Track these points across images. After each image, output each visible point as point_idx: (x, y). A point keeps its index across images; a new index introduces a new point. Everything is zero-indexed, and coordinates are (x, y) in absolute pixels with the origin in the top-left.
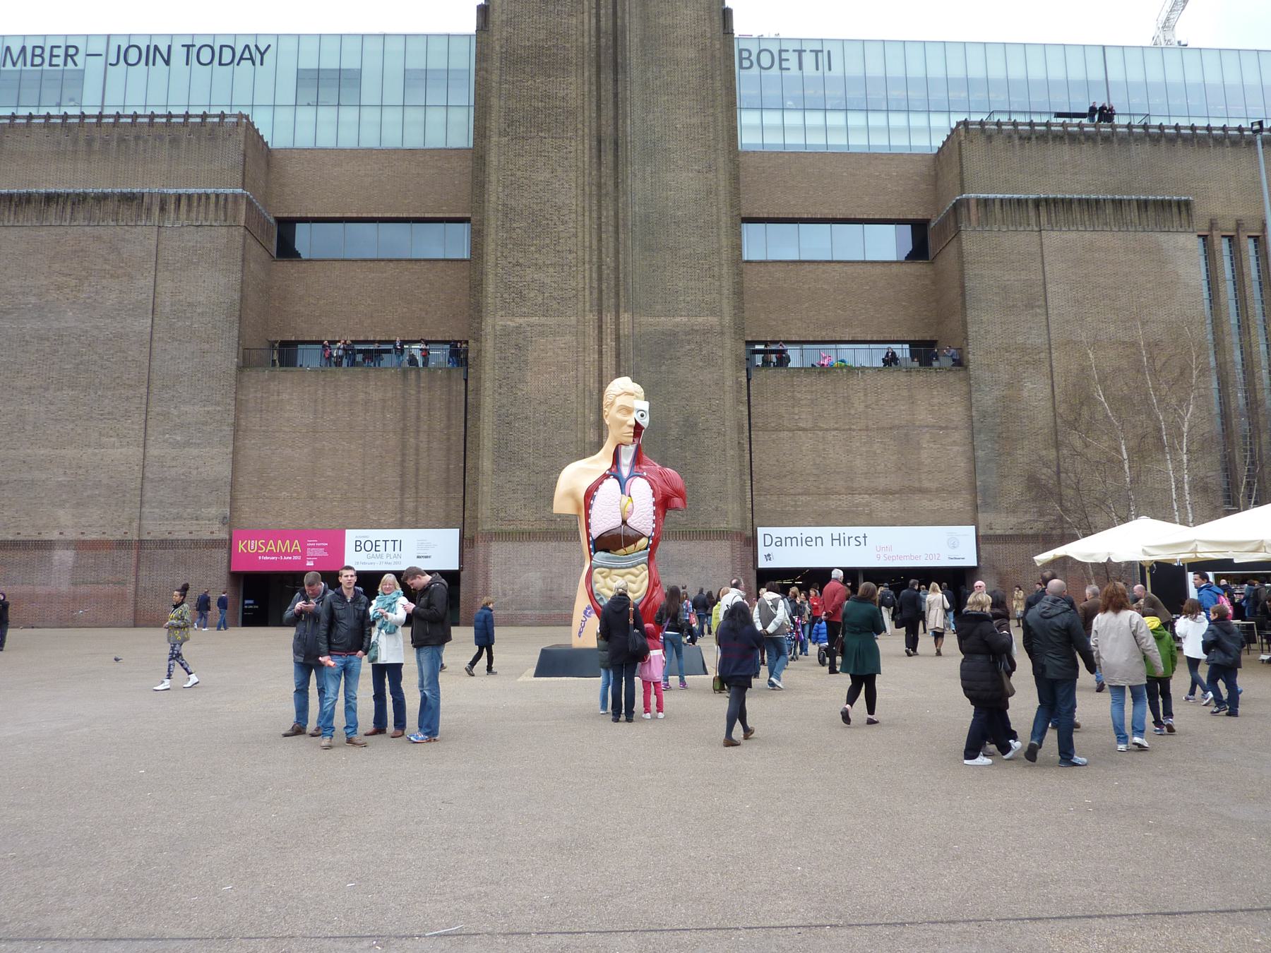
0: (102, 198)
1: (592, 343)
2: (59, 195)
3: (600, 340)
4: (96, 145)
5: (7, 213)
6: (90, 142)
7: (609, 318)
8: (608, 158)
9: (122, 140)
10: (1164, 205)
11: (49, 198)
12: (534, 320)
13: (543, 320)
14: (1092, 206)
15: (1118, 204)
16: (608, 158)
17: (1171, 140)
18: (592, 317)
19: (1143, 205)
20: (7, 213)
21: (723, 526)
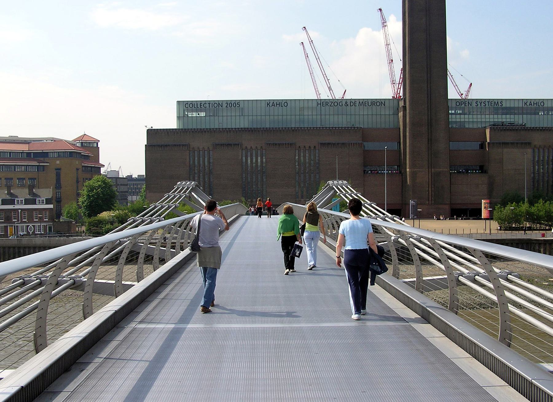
0: (338, 144)
1: (427, 174)
3: (429, 173)
7: (430, 170)
8: (430, 142)
10: (526, 143)
11: (329, 144)
12: (418, 170)
13: (419, 170)
14: (512, 143)
15: (517, 143)
16: (430, 142)
17: (529, 130)
18: (427, 169)
19: (522, 143)
21: (447, 203)
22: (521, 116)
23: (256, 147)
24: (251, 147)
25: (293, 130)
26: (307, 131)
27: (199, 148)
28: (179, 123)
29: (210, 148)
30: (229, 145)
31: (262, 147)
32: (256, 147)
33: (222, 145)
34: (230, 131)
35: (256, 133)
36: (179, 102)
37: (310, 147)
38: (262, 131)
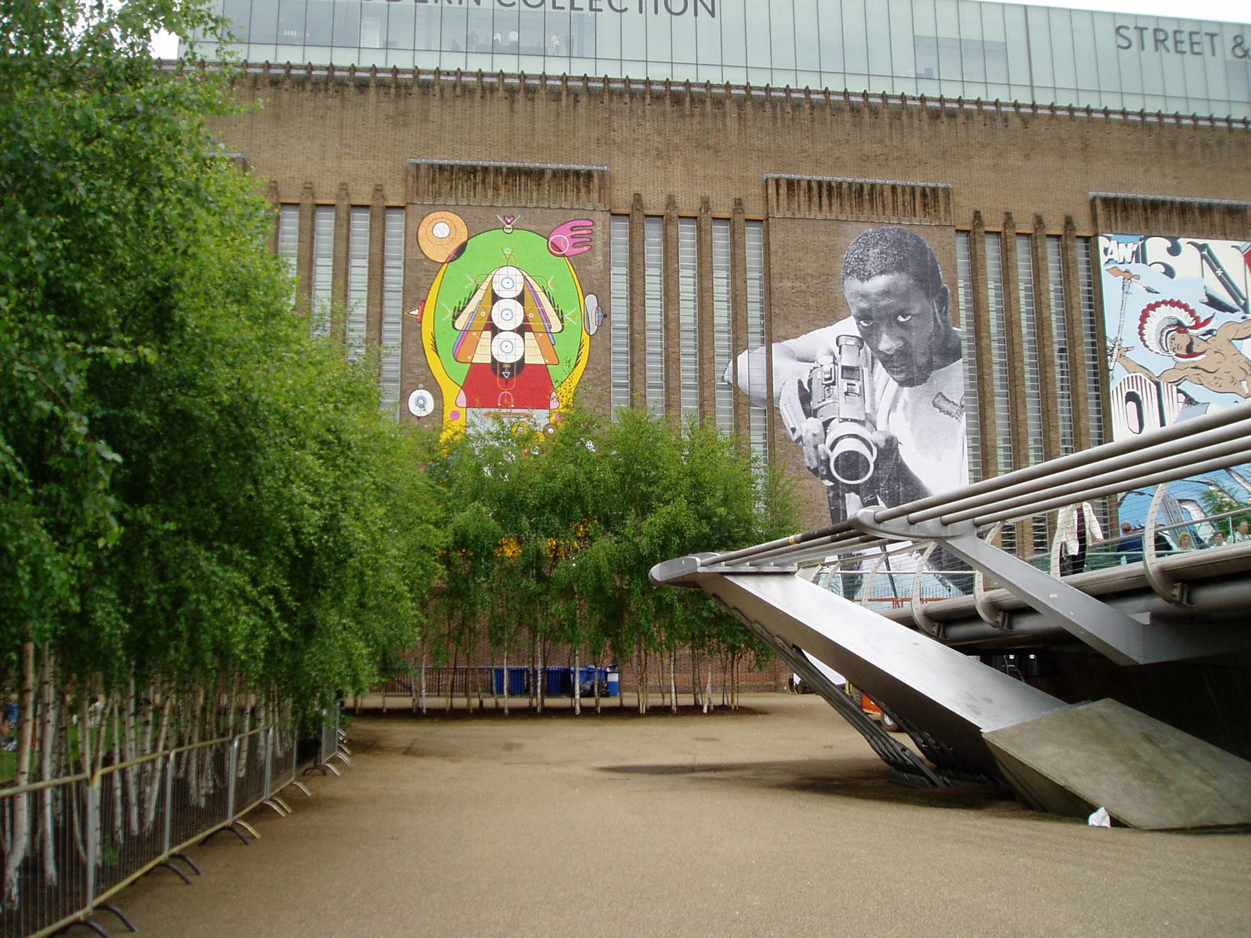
0: (1206, 210)
2: (1164, 203)
4: (1181, 148)
5: (1113, 218)
6: (1173, 145)
9: (1205, 146)
11: (1154, 206)
20: (1113, 218)
23: (706, 204)
24: (671, 202)
25: (935, 115)
26: (1017, 121)
27: (309, 189)
29: (388, 190)
30: (514, 173)
31: (738, 203)
32: (706, 204)
33: (470, 172)
34: (530, 91)
35: (703, 115)
37: (1039, 221)
38: (741, 102)
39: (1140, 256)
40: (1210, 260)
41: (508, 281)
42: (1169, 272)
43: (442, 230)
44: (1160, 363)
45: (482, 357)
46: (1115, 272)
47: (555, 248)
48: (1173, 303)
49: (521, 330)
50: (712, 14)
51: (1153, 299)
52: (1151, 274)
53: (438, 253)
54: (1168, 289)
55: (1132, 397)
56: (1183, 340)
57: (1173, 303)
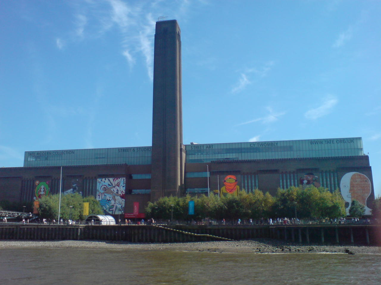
11: (104, 175)
15: (230, 172)
22: (240, 154)
28: (24, 165)
36: (26, 152)
39: (102, 181)
40: (109, 180)
41: (42, 187)
42: (105, 182)
43: (37, 182)
44: (102, 192)
45: (40, 194)
46: (99, 182)
47: (47, 184)
48: (105, 185)
49: (43, 191)
50: (74, 153)
51: (102, 185)
52: (102, 182)
53: (37, 185)
54: (104, 184)
55: (99, 195)
56: (105, 189)
57: (105, 185)
